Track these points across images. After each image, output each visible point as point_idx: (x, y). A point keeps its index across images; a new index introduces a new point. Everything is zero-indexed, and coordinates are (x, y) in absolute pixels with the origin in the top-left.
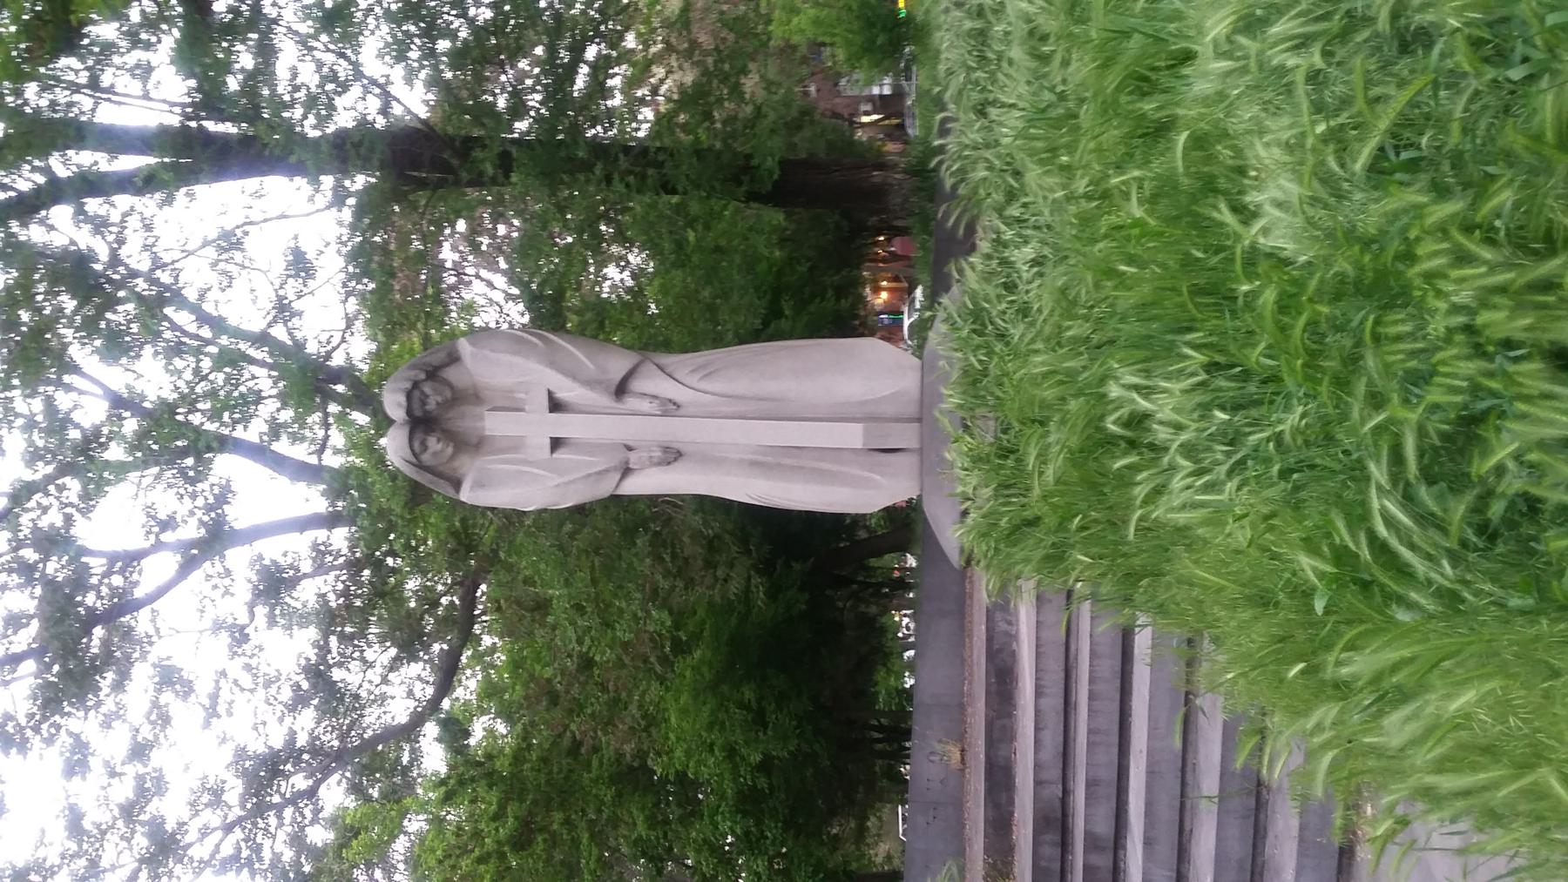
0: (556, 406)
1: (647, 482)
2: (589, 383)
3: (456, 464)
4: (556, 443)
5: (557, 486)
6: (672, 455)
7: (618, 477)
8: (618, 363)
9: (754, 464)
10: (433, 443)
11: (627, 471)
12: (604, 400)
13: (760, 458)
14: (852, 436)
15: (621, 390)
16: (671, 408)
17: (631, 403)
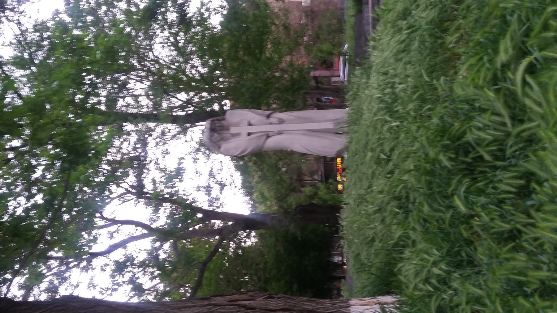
0: (250, 125)
1: (273, 143)
2: (260, 115)
3: (220, 143)
4: (249, 134)
5: (250, 139)
6: (280, 133)
7: (264, 137)
8: (268, 112)
9: (303, 134)
10: (216, 135)
11: (268, 137)
12: (263, 119)
13: (305, 133)
14: (329, 126)
15: (268, 116)
16: (281, 122)
17: (272, 120)
